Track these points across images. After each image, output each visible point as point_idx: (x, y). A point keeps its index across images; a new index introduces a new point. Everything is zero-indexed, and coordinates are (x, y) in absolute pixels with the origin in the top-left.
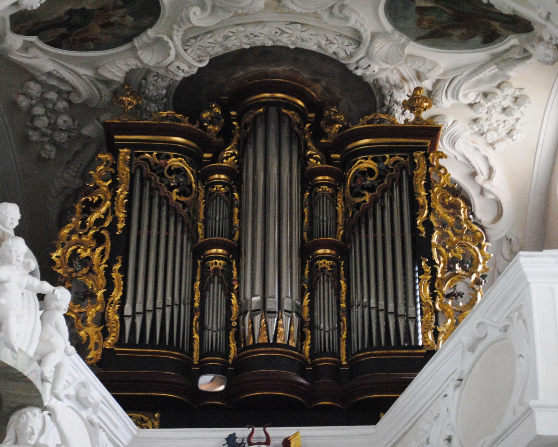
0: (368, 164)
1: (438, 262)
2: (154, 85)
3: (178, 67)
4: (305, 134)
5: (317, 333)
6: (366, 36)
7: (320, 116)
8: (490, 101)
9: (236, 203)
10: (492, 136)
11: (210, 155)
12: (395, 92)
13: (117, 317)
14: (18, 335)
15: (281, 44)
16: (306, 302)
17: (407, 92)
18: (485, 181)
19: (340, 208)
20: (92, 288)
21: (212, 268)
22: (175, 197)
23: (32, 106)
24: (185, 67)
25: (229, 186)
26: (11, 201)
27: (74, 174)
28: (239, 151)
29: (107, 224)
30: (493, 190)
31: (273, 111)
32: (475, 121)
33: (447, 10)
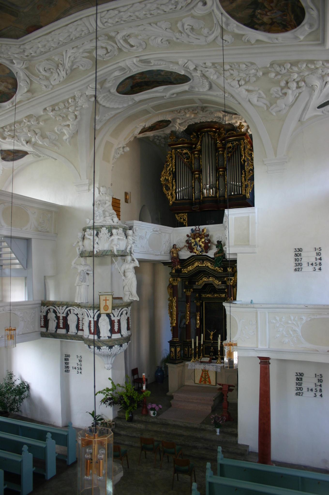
0: (230, 145)
1: (246, 171)
11: (194, 146)
16: (217, 183)
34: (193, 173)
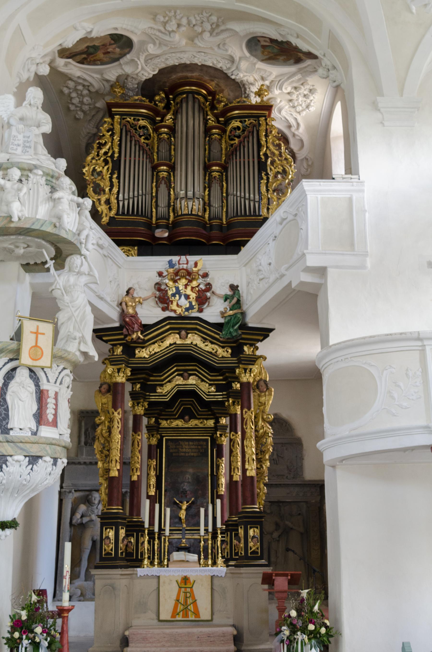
1: (270, 174)
2: (131, 82)
3: (143, 74)
4: (206, 108)
5: (212, 208)
6: (237, 59)
7: (214, 99)
8: (298, 91)
9: (173, 143)
10: (299, 108)
12: (251, 87)
13: (116, 201)
14: (68, 223)
15: (194, 63)
16: (207, 193)
17: (257, 86)
18: (295, 130)
19: (223, 146)
20: (103, 187)
21: (161, 176)
22: (143, 141)
23: (70, 93)
24: (146, 74)
25: (169, 135)
26: (62, 157)
27: (93, 126)
28: (174, 116)
29: (109, 154)
30: (299, 134)
31: (190, 96)
32: (291, 101)
33: (276, 47)
34: (154, 168)
